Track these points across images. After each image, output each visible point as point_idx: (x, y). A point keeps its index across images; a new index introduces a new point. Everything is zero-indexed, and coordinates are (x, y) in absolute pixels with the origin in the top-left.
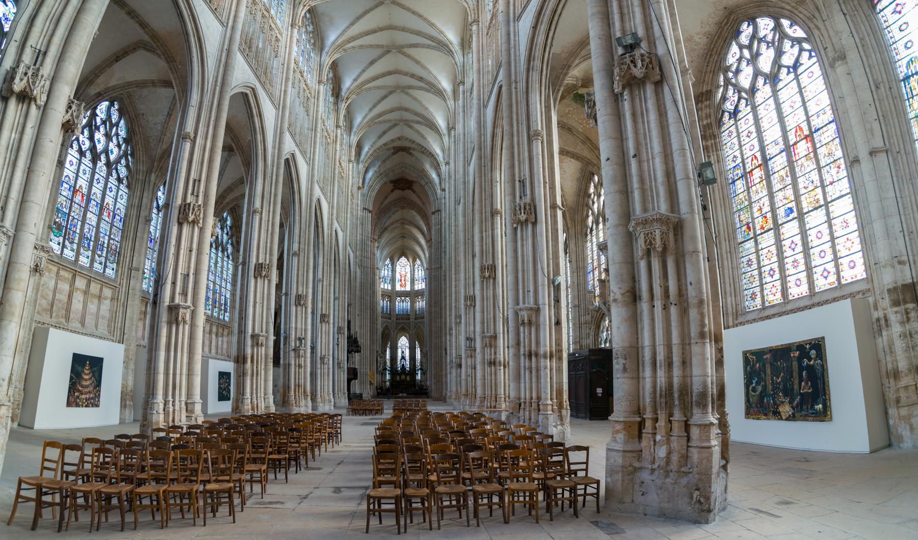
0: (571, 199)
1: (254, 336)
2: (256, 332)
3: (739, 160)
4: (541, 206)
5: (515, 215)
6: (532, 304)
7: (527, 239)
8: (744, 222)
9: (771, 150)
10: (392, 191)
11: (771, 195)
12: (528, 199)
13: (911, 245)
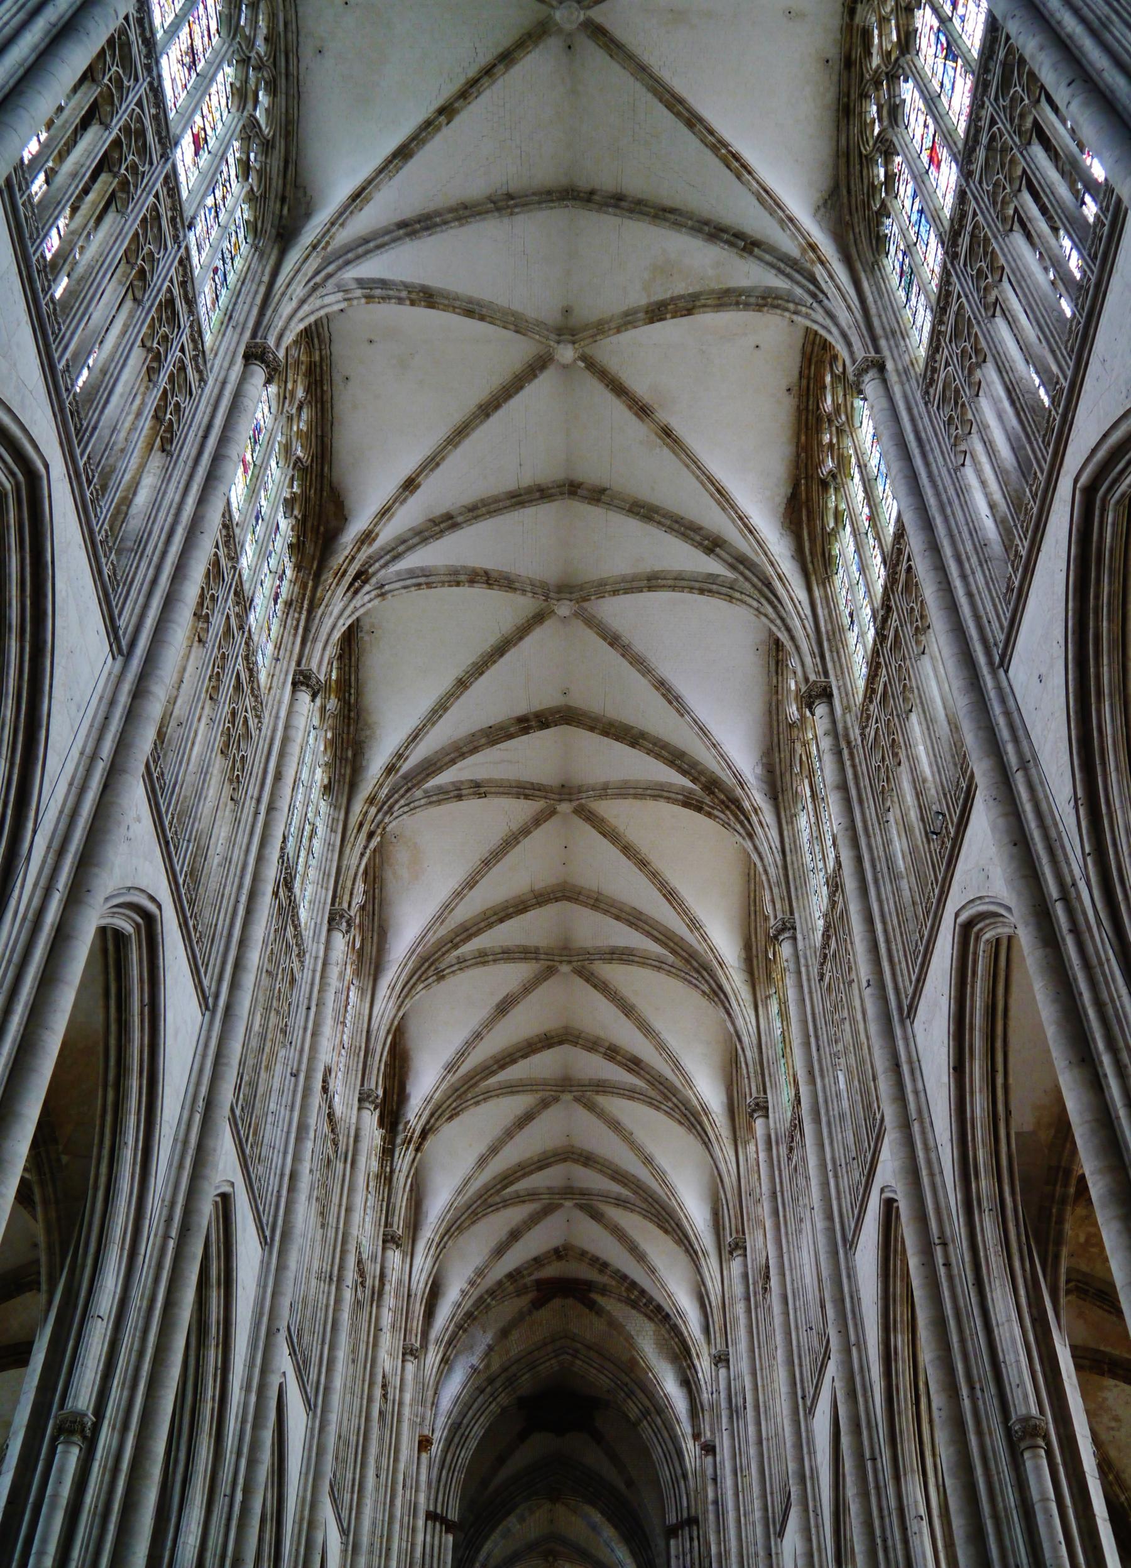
10: (523, 1436)
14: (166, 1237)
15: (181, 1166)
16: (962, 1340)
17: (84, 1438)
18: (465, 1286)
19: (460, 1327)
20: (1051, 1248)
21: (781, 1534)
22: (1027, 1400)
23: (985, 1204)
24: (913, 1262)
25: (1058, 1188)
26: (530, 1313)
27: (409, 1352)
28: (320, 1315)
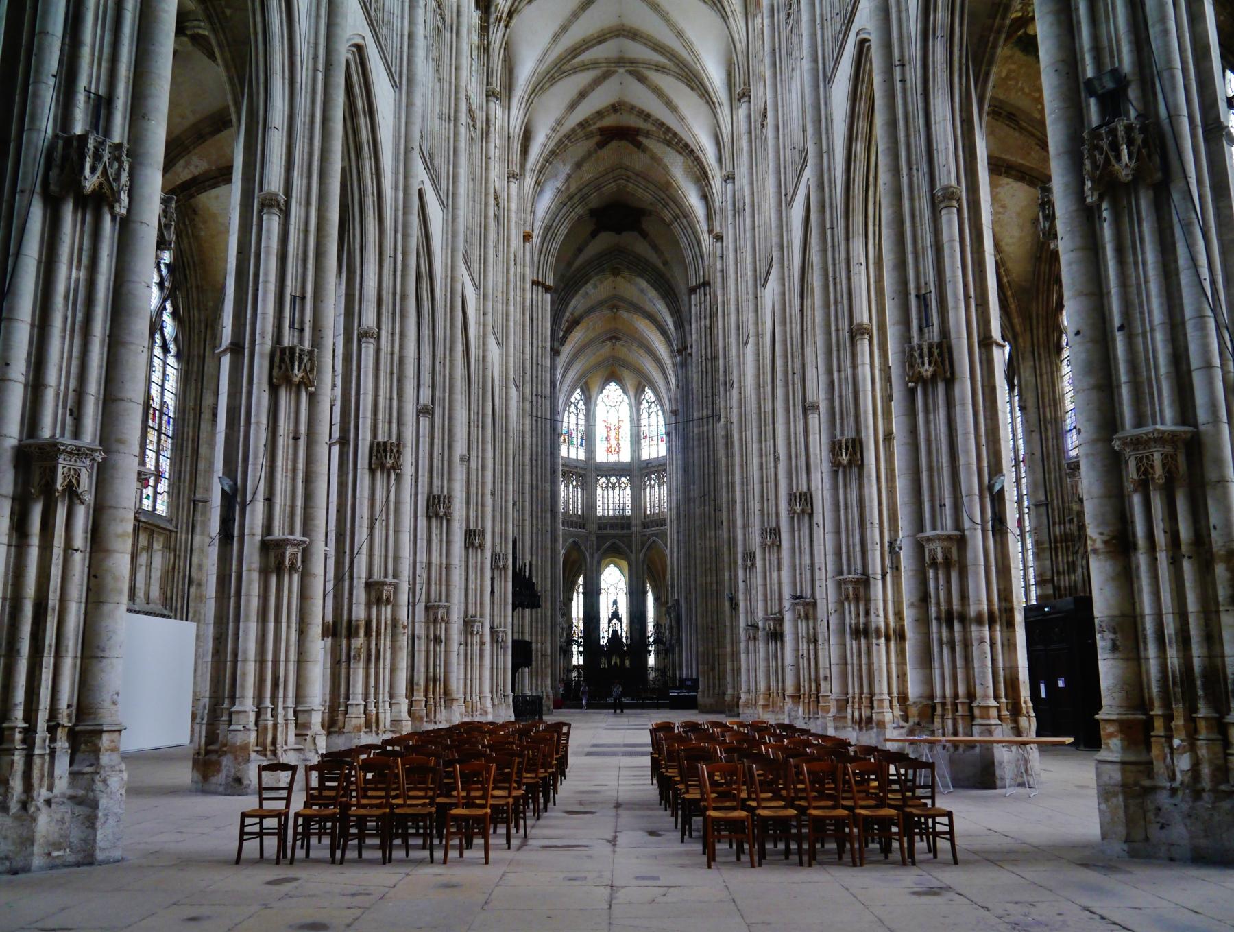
0: (1018, 269)
1: (369, 585)
2: (376, 577)
4: (960, 346)
5: (912, 366)
6: (949, 529)
7: (935, 409)
10: (594, 235)
12: (934, 334)
14: (315, 70)
15: (318, 16)
16: (908, 136)
17: (281, 210)
18: (549, 132)
19: (547, 161)
20: (984, 68)
21: (764, 285)
22: (949, 173)
23: (938, 32)
24: (877, 80)
25: (997, 20)
26: (596, 151)
27: (511, 176)
28: (445, 144)
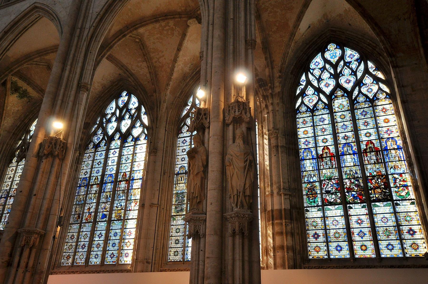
3: (88, 175)
8: (77, 213)
9: (107, 179)
11: (98, 203)
13: (156, 254)
